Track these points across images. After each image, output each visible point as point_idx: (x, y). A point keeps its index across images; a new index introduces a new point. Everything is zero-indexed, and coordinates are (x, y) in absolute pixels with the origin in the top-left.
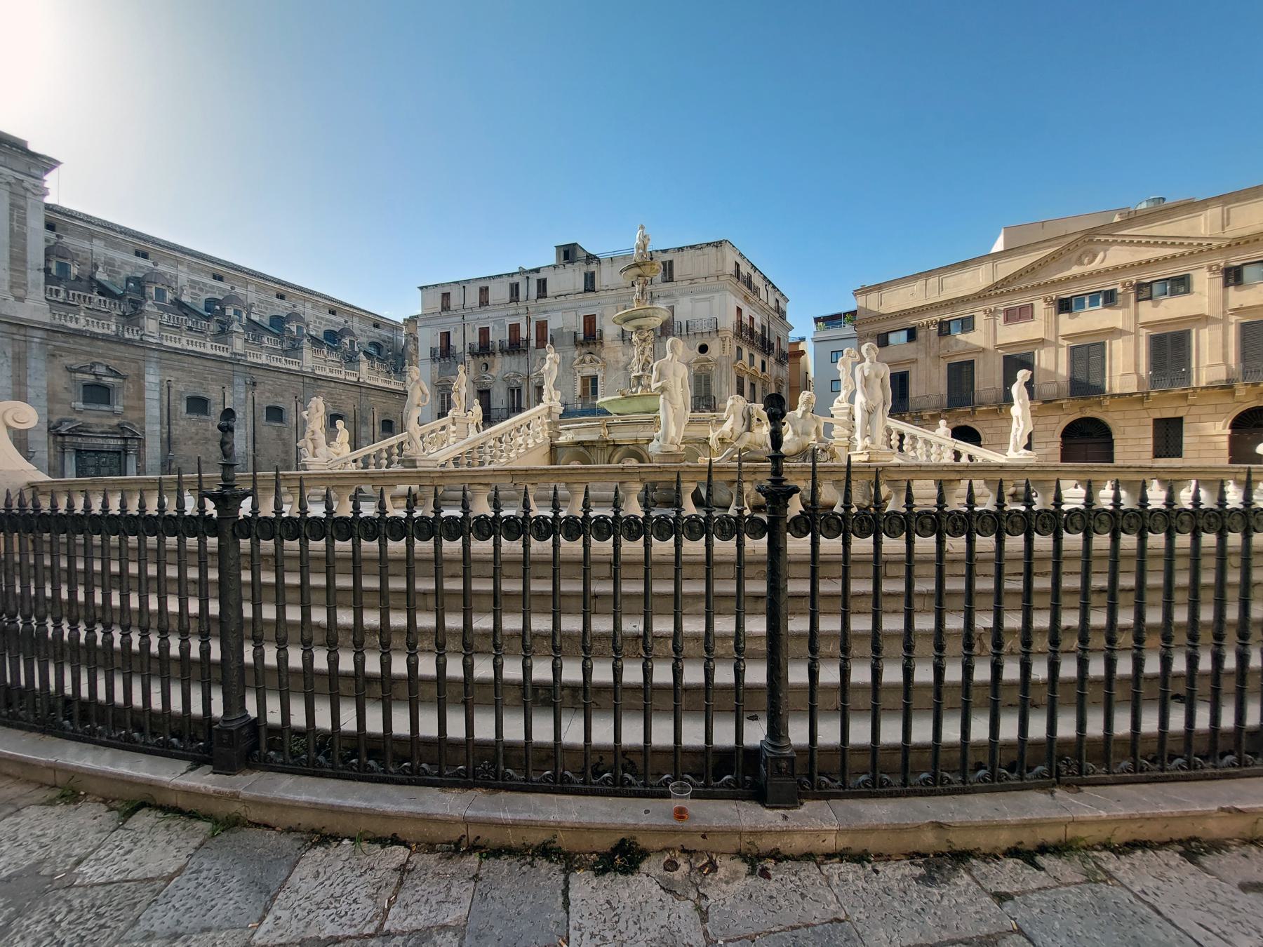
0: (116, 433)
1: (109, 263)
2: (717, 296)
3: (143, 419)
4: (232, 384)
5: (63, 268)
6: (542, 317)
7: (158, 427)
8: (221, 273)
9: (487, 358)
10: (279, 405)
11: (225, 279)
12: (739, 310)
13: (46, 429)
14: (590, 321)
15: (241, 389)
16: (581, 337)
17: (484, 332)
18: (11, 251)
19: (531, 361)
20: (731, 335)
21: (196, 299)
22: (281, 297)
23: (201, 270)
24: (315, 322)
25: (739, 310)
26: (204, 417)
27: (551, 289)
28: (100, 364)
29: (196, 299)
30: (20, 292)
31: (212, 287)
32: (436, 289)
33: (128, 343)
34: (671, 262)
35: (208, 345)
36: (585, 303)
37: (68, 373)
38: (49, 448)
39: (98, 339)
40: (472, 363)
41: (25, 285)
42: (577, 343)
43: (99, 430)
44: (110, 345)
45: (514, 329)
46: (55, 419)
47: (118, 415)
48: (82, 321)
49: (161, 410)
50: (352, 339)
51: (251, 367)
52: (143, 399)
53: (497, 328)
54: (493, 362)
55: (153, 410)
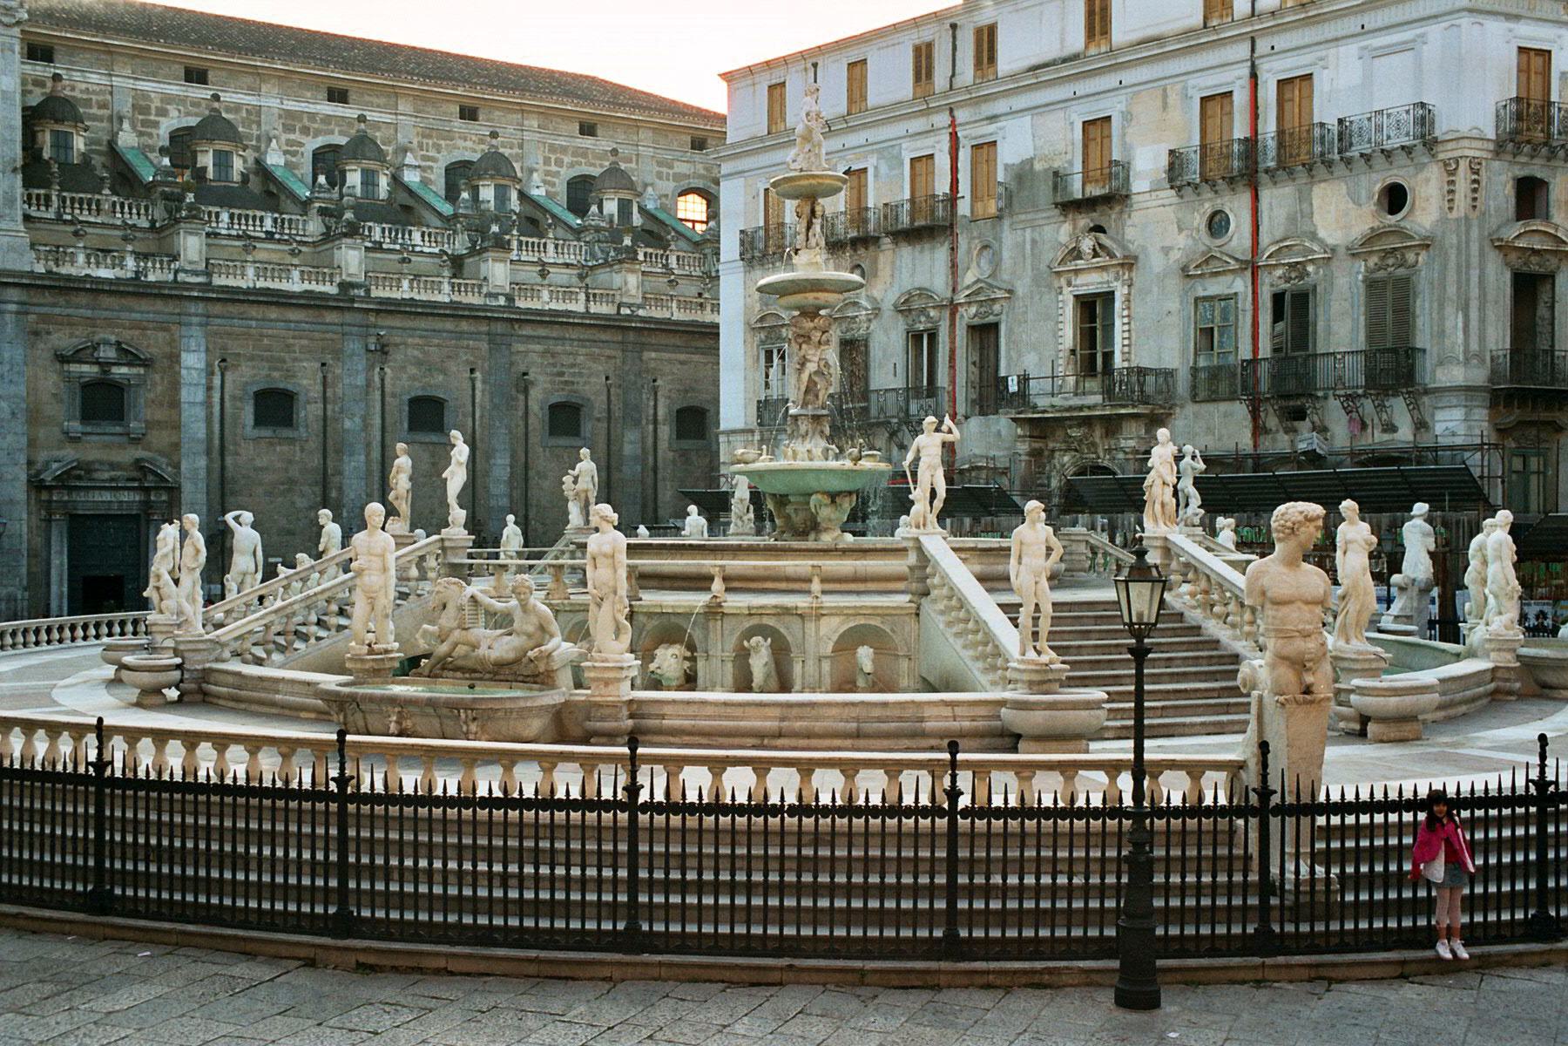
0: (133, 480)
1: (141, 108)
2: (1434, 31)
3: (176, 446)
4: (338, 354)
5: (62, 142)
6: (987, 131)
7: (202, 462)
8: (341, 85)
9: (862, 251)
11: (352, 96)
13: (24, 477)
14: (1096, 128)
15: (361, 364)
21: (294, 154)
22: (468, 113)
23: (308, 82)
24: (547, 161)
26: (286, 433)
28: (107, 343)
29: (294, 154)
31: (328, 119)
32: (757, 78)
33: (156, 292)
35: (296, 274)
36: (1083, 87)
37: (58, 366)
38: (29, 513)
39: (104, 291)
42: (1071, 207)
43: (106, 475)
44: (125, 302)
46: (42, 456)
47: (136, 441)
50: (626, 195)
51: (378, 312)
52: (175, 404)
53: (883, 169)
54: (875, 261)
55: (195, 424)
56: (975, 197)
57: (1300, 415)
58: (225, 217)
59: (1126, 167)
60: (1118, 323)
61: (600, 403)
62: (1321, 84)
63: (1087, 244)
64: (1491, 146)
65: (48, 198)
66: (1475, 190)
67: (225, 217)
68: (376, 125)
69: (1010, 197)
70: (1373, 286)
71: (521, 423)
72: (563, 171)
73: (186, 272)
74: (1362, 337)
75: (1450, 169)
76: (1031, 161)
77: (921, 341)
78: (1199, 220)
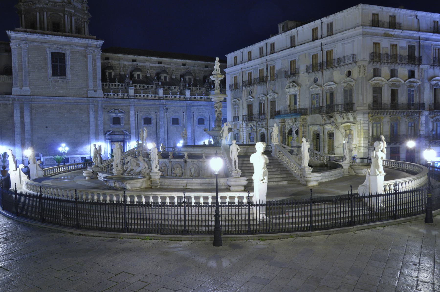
1: (125, 67)
3: (130, 128)
5: (110, 74)
7: (134, 131)
9: (251, 88)
10: (178, 117)
11: (162, 63)
12: (377, 45)
14: (293, 63)
16: (289, 73)
17: (250, 74)
18: (93, 76)
19: (268, 88)
20: (366, 63)
24: (199, 73)
25: (377, 45)
27: (276, 48)
30: (95, 89)
34: (331, 24)
40: (246, 91)
41: (97, 86)
45: (261, 71)
46: (106, 131)
48: (112, 95)
49: (135, 123)
52: (129, 120)
54: (253, 89)
56: (271, 76)
57: (331, 117)
58: (138, 86)
59: (298, 69)
60: (297, 100)
61: (208, 117)
62: (335, 52)
63: (291, 85)
64: (368, 62)
65: (107, 84)
66: (364, 72)
67: (138, 86)
68: (167, 68)
69: (277, 76)
70: (345, 91)
71: (193, 122)
72: (202, 74)
73: (130, 96)
74: (343, 100)
75: (359, 67)
76: (281, 69)
77: (262, 105)
78: (312, 79)
